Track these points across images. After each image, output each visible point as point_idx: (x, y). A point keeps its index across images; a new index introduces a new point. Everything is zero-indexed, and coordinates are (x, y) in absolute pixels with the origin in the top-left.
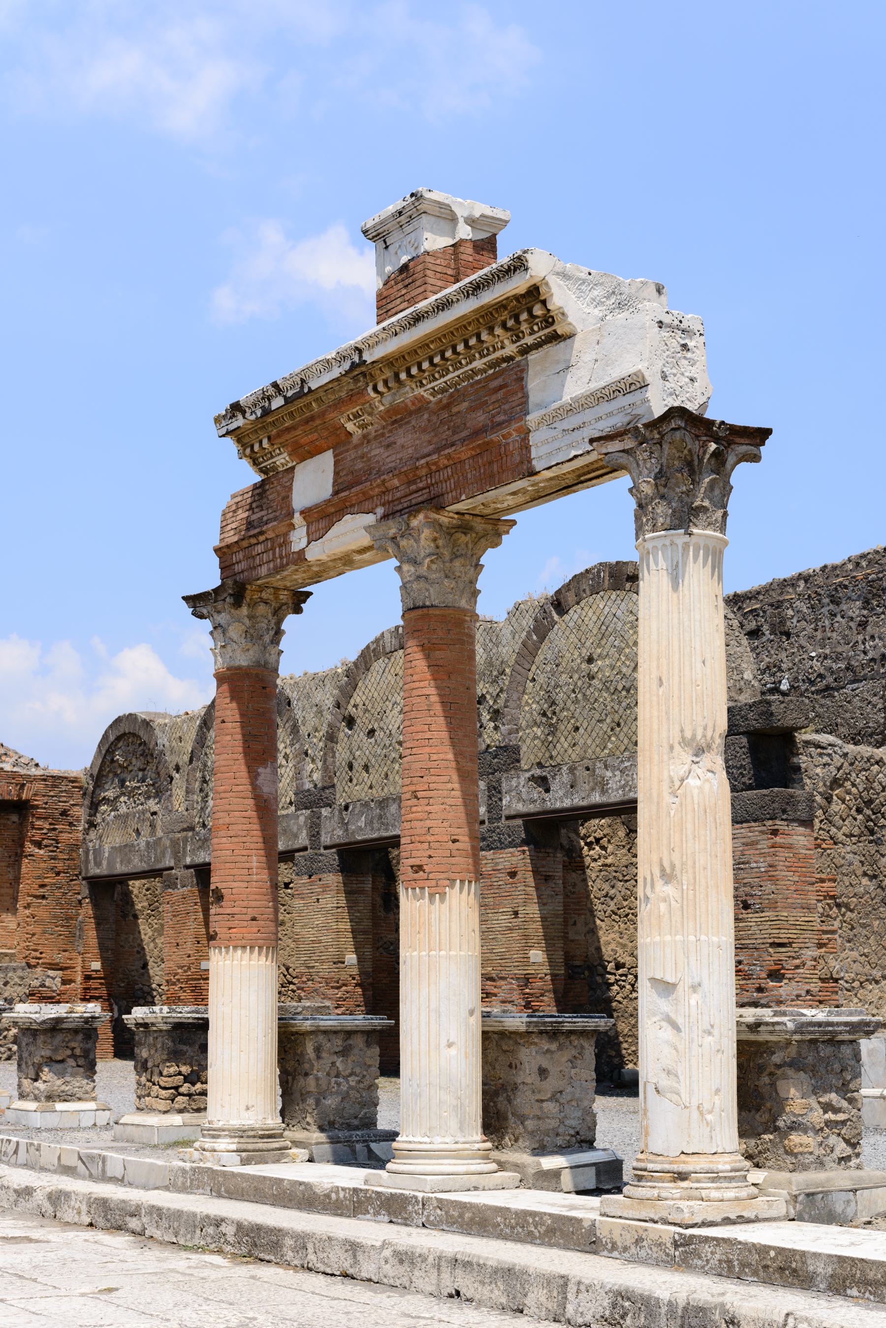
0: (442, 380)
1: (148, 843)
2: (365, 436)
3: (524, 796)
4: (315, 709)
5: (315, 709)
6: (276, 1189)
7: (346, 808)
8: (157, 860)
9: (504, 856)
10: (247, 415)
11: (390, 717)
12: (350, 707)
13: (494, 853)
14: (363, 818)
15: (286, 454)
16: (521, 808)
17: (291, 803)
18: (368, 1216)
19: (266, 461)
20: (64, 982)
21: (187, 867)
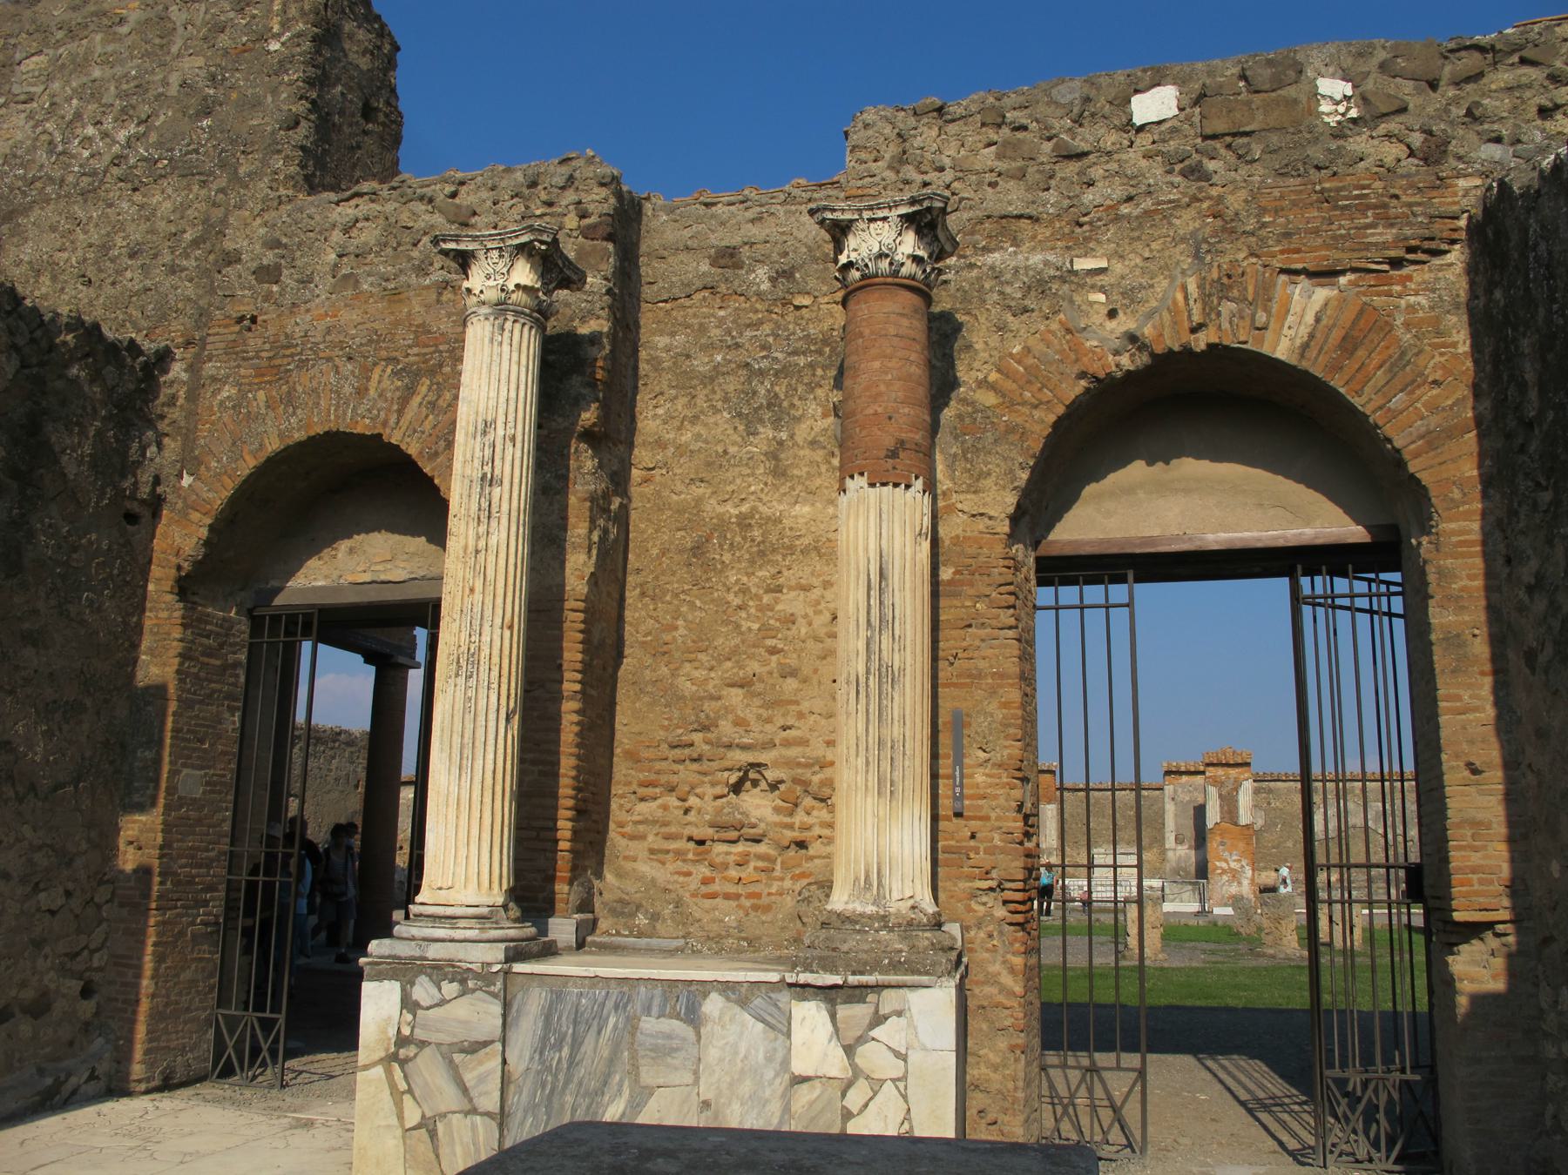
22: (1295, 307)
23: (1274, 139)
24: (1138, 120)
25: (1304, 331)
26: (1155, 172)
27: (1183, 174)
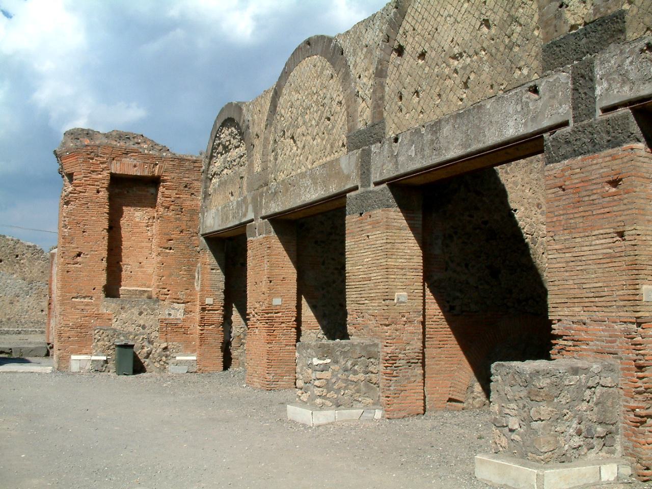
1: (238, 202)
3: (632, 76)
4: (365, 49)
5: (365, 49)
7: (396, 140)
8: (245, 215)
9: (600, 160)
11: (442, 34)
12: (399, 37)
13: (582, 160)
14: (413, 148)
16: (627, 93)
17: (343, 145)
20: (186, 312)
21: (263, 218)
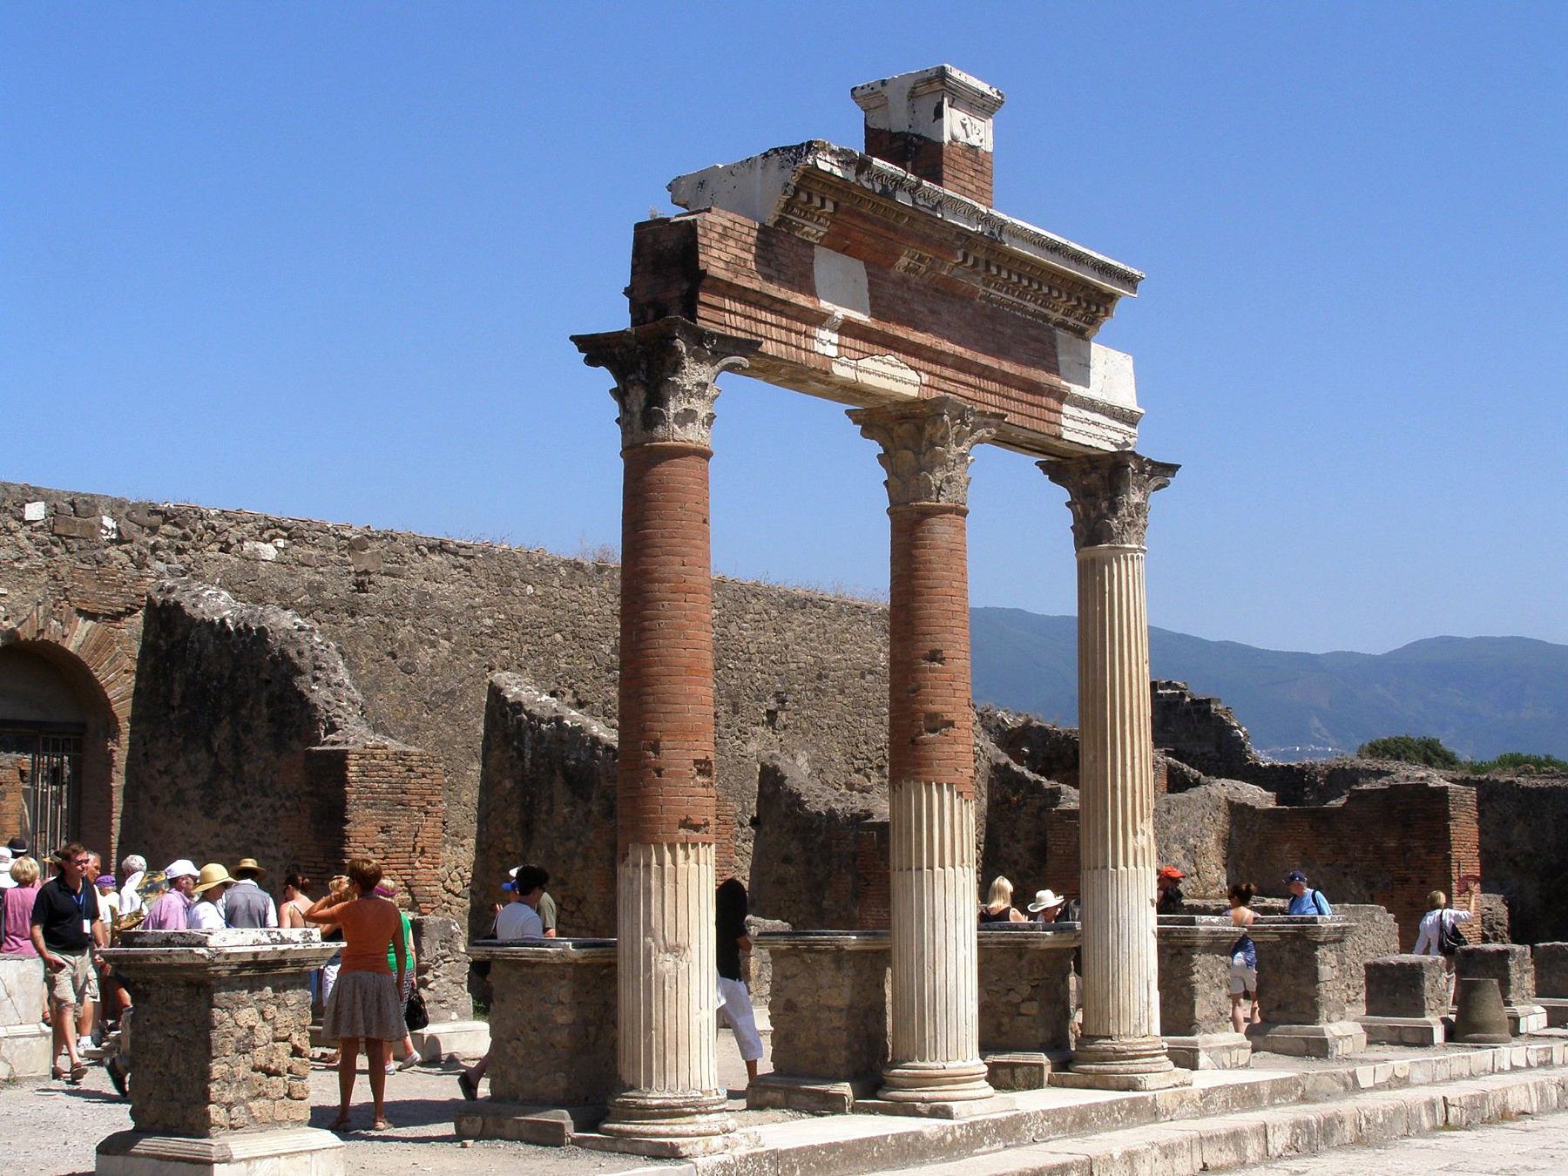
0: (1002, 295)
2: (905, 280)
6: (878, 1150)
10: (863, 178)
15: (826, 230)
18: (985, 1149)
19: (799, 217)
22: (79, 627)
23: (83, 543)
24: (27, 517)
25: (81, 639)
26: (31, 549)
27: (43, 552)
